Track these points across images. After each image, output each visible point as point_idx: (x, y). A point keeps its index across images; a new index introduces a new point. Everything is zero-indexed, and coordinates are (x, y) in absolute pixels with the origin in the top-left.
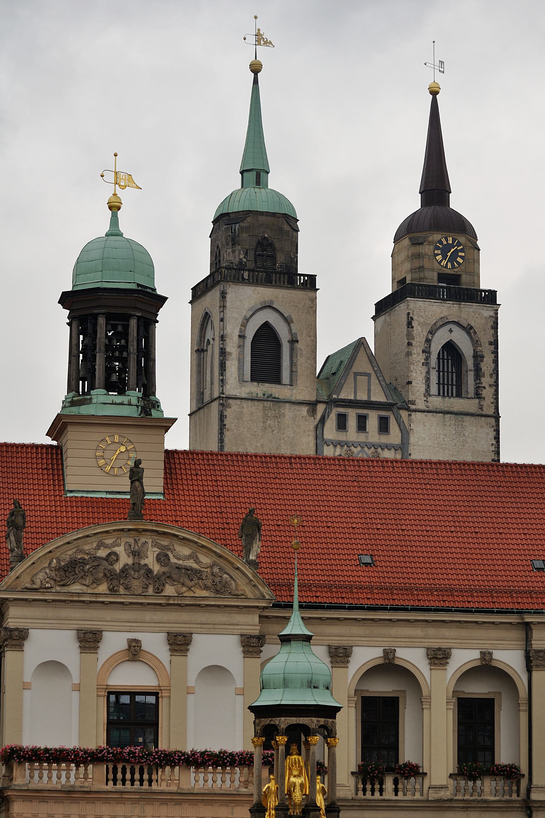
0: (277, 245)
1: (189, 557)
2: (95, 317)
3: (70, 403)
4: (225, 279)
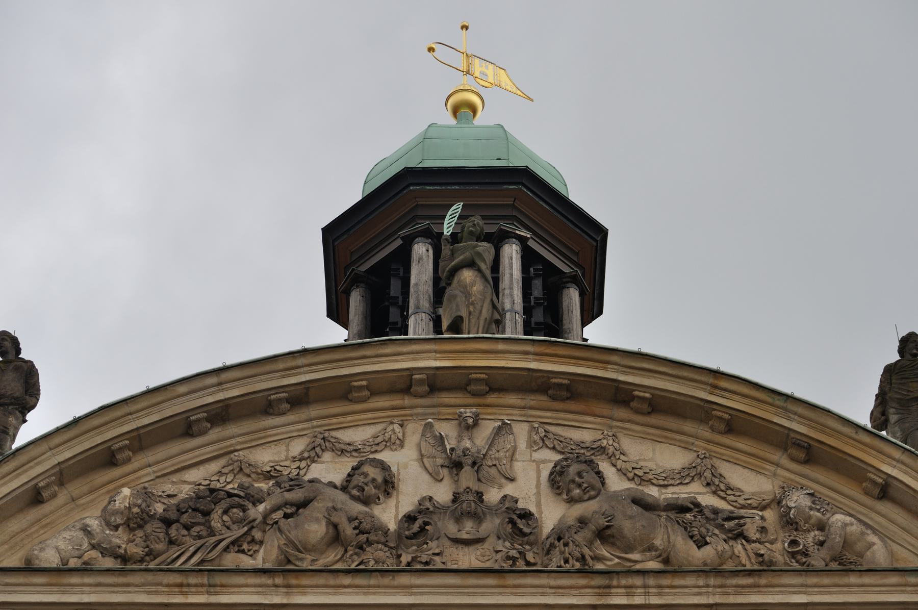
1: (686, 475)
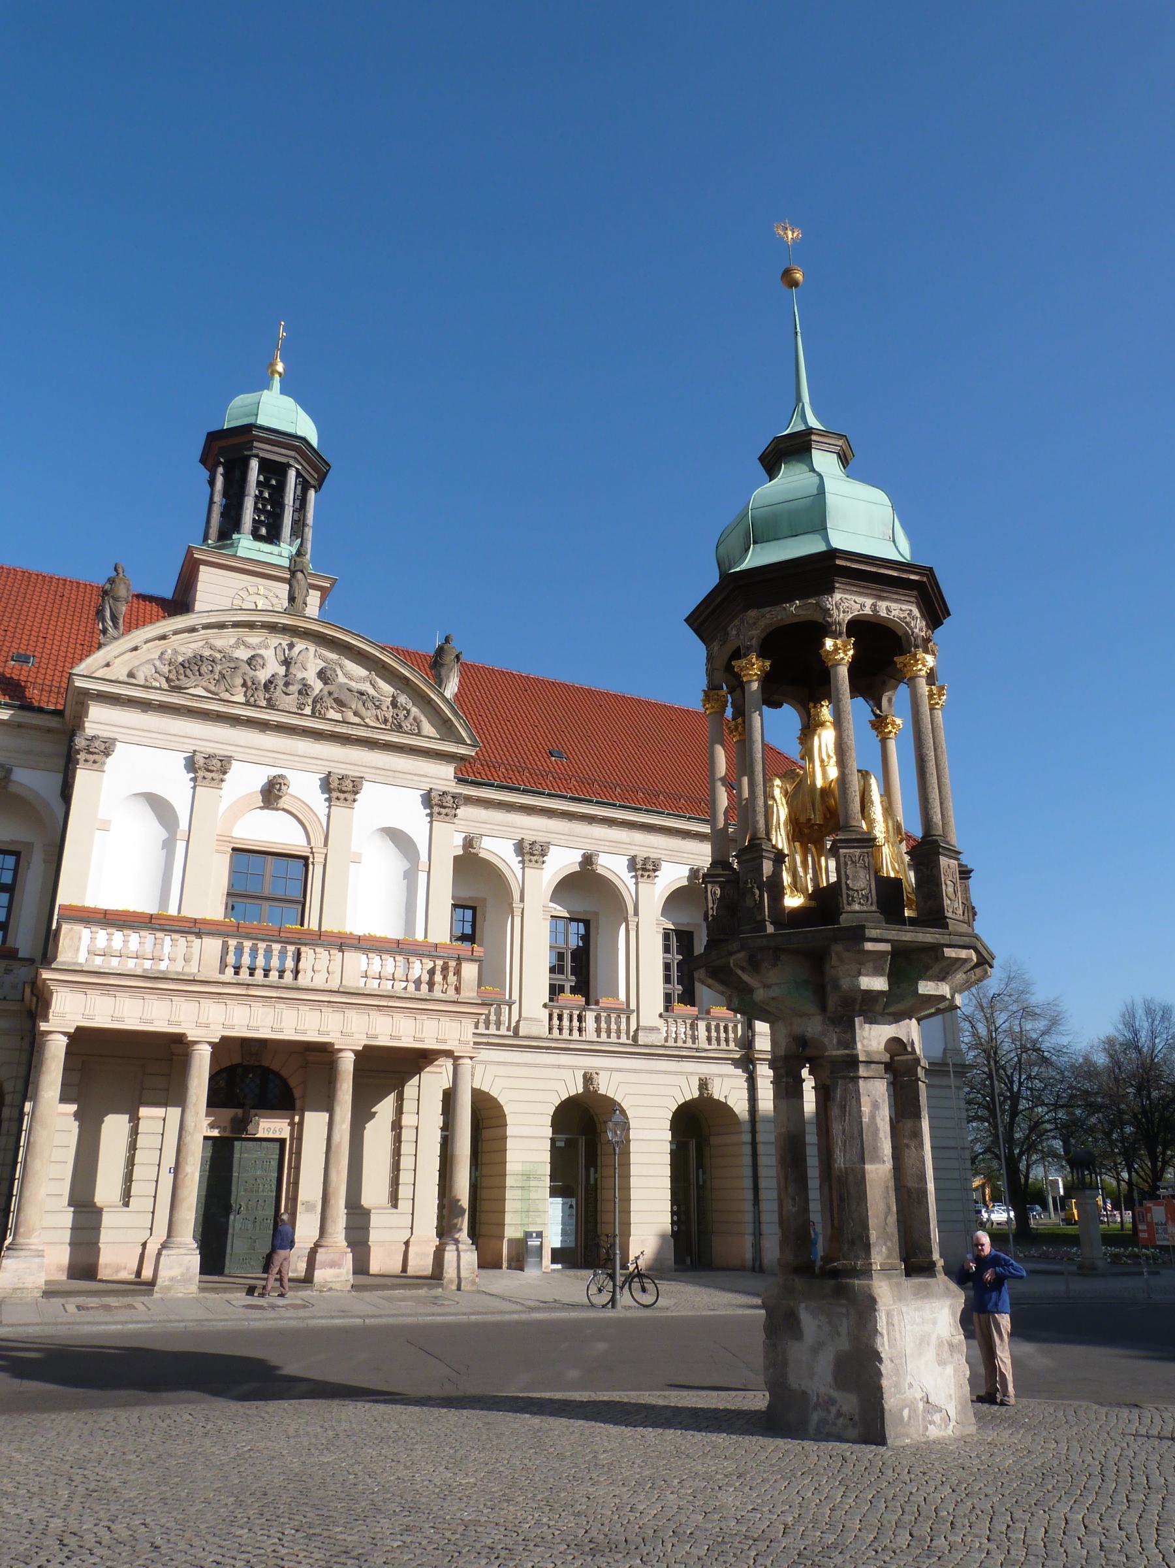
1: (364, 680)
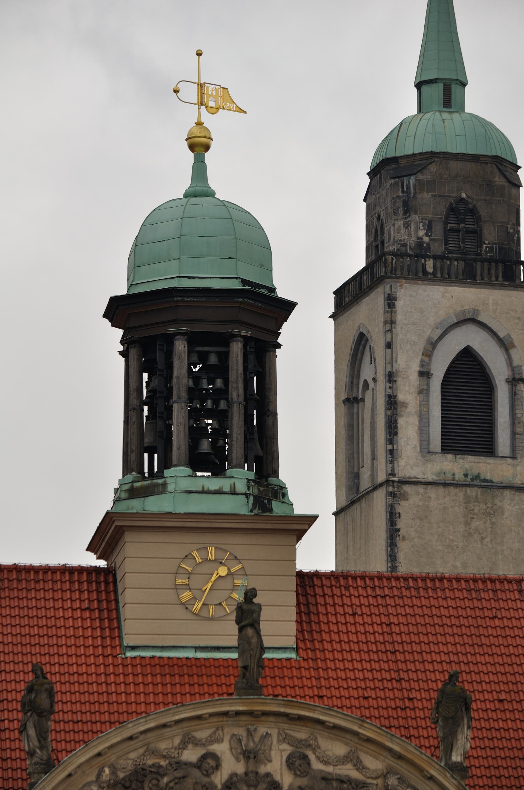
0: (483, 211)
2: (169, 339)
3: (128, 492)
4: (393, 274)
